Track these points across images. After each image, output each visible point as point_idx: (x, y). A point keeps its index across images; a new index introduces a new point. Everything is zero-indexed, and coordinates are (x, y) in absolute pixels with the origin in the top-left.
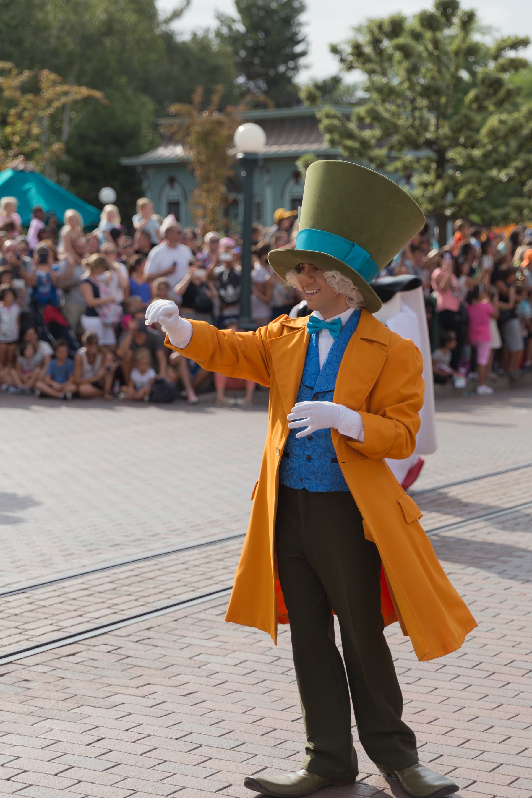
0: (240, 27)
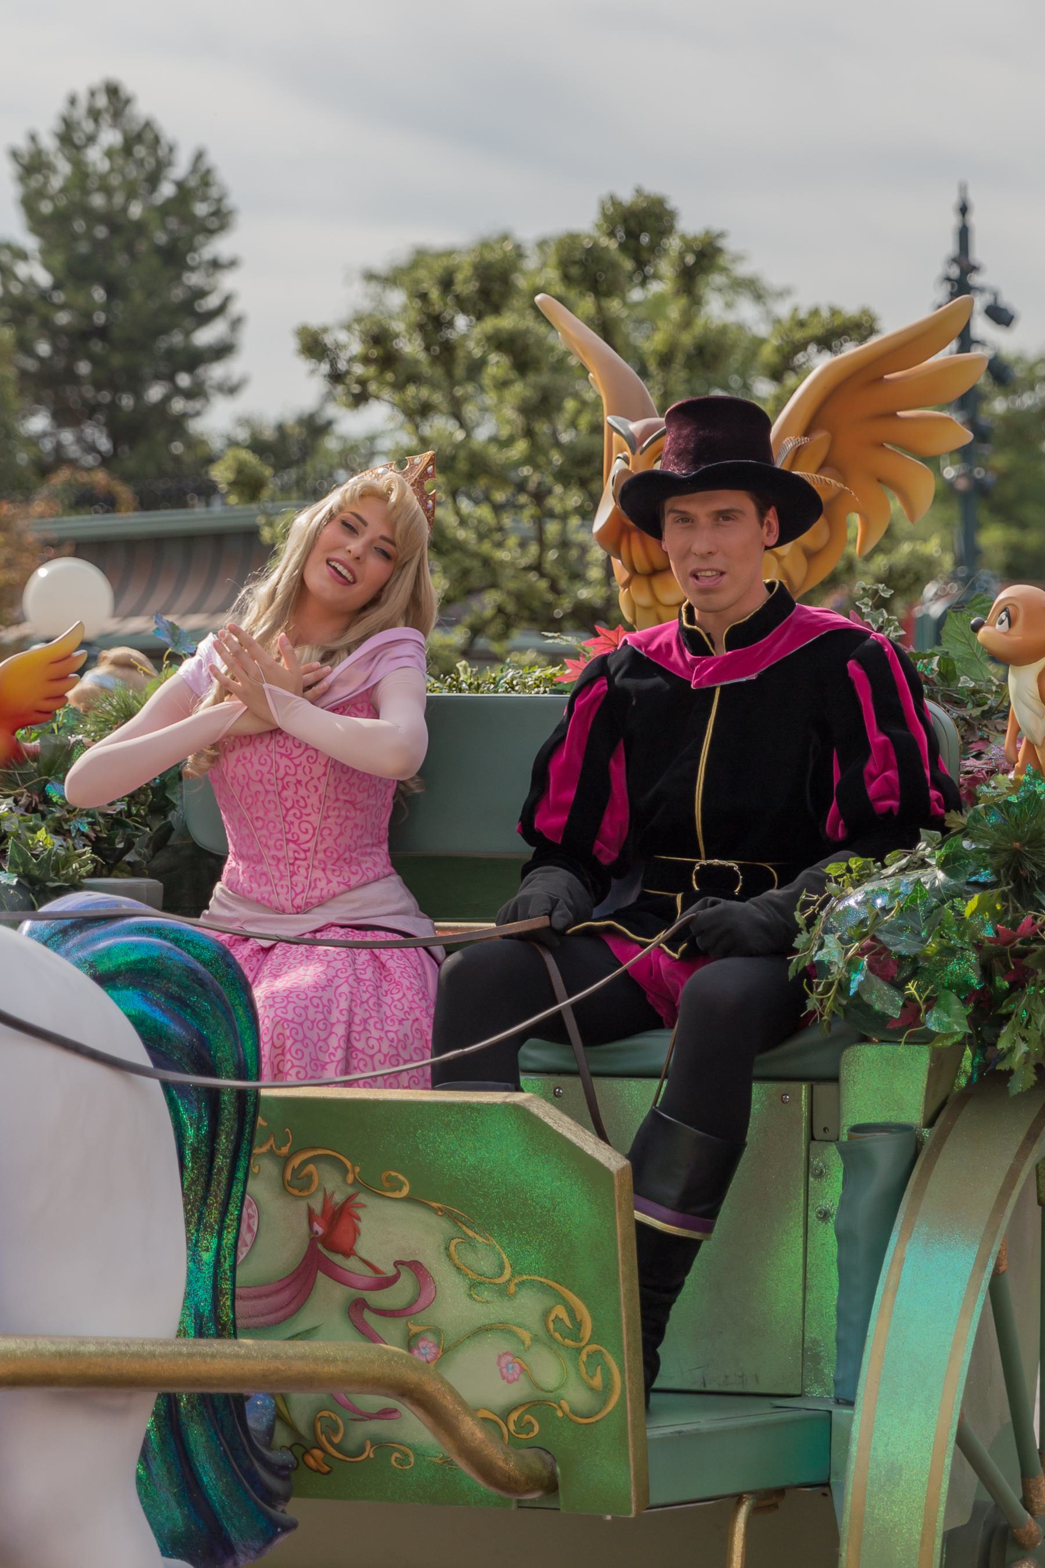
0: (37, 273)
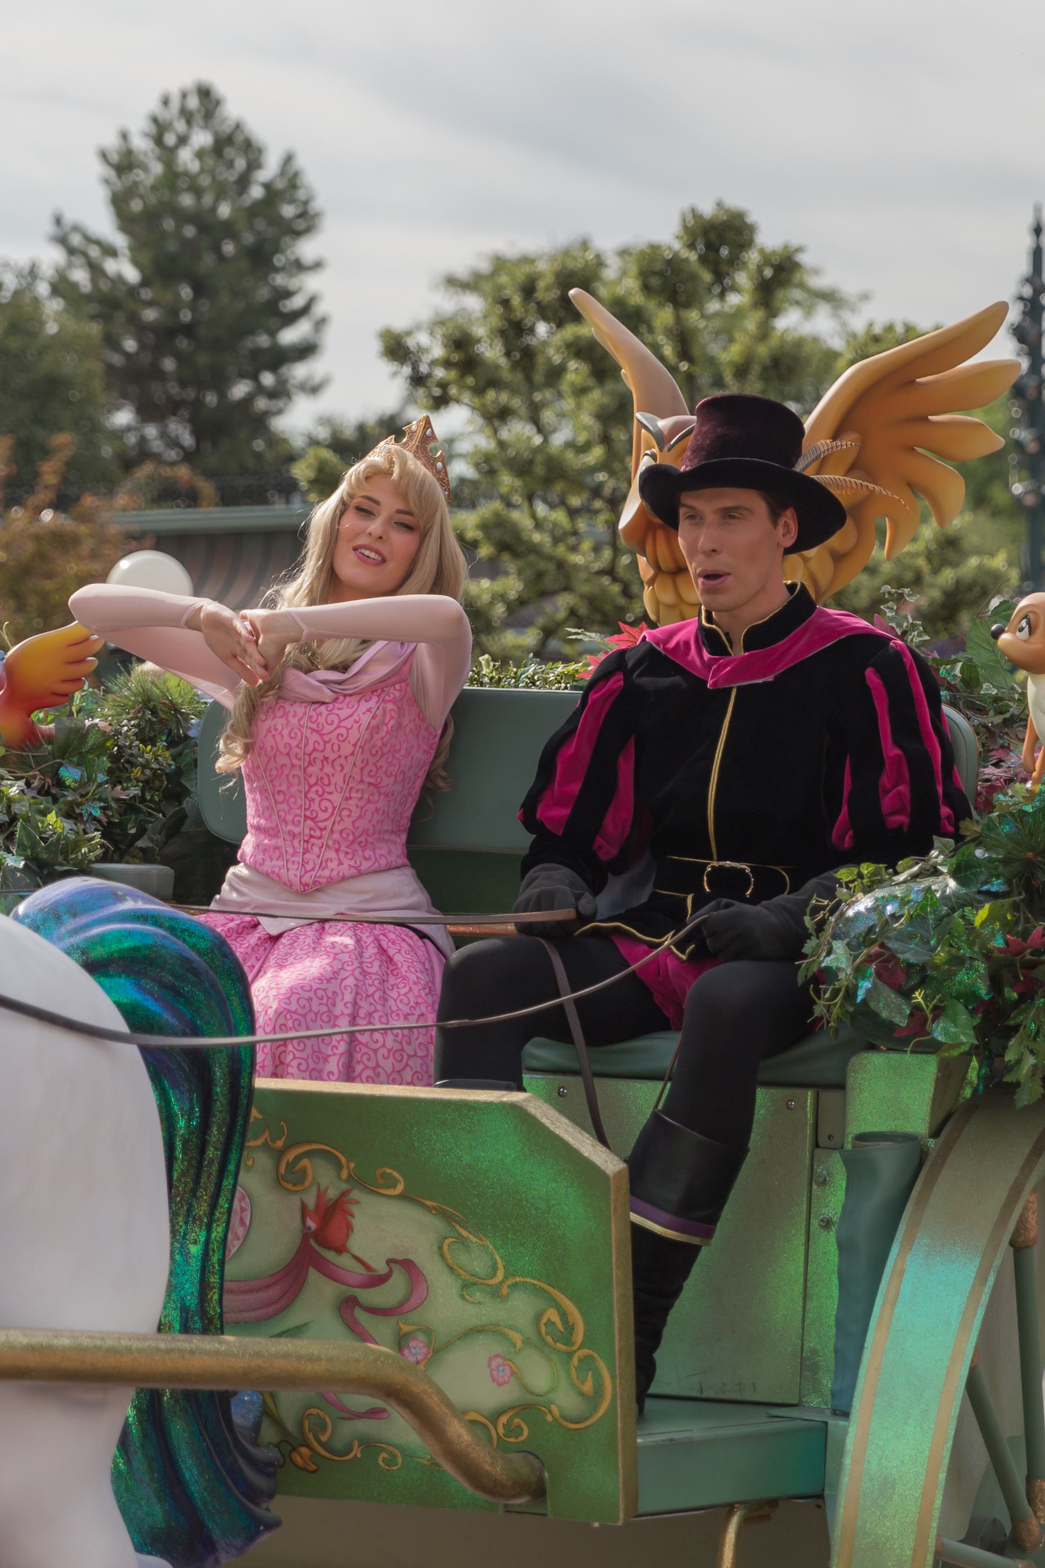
0: (126, 270)
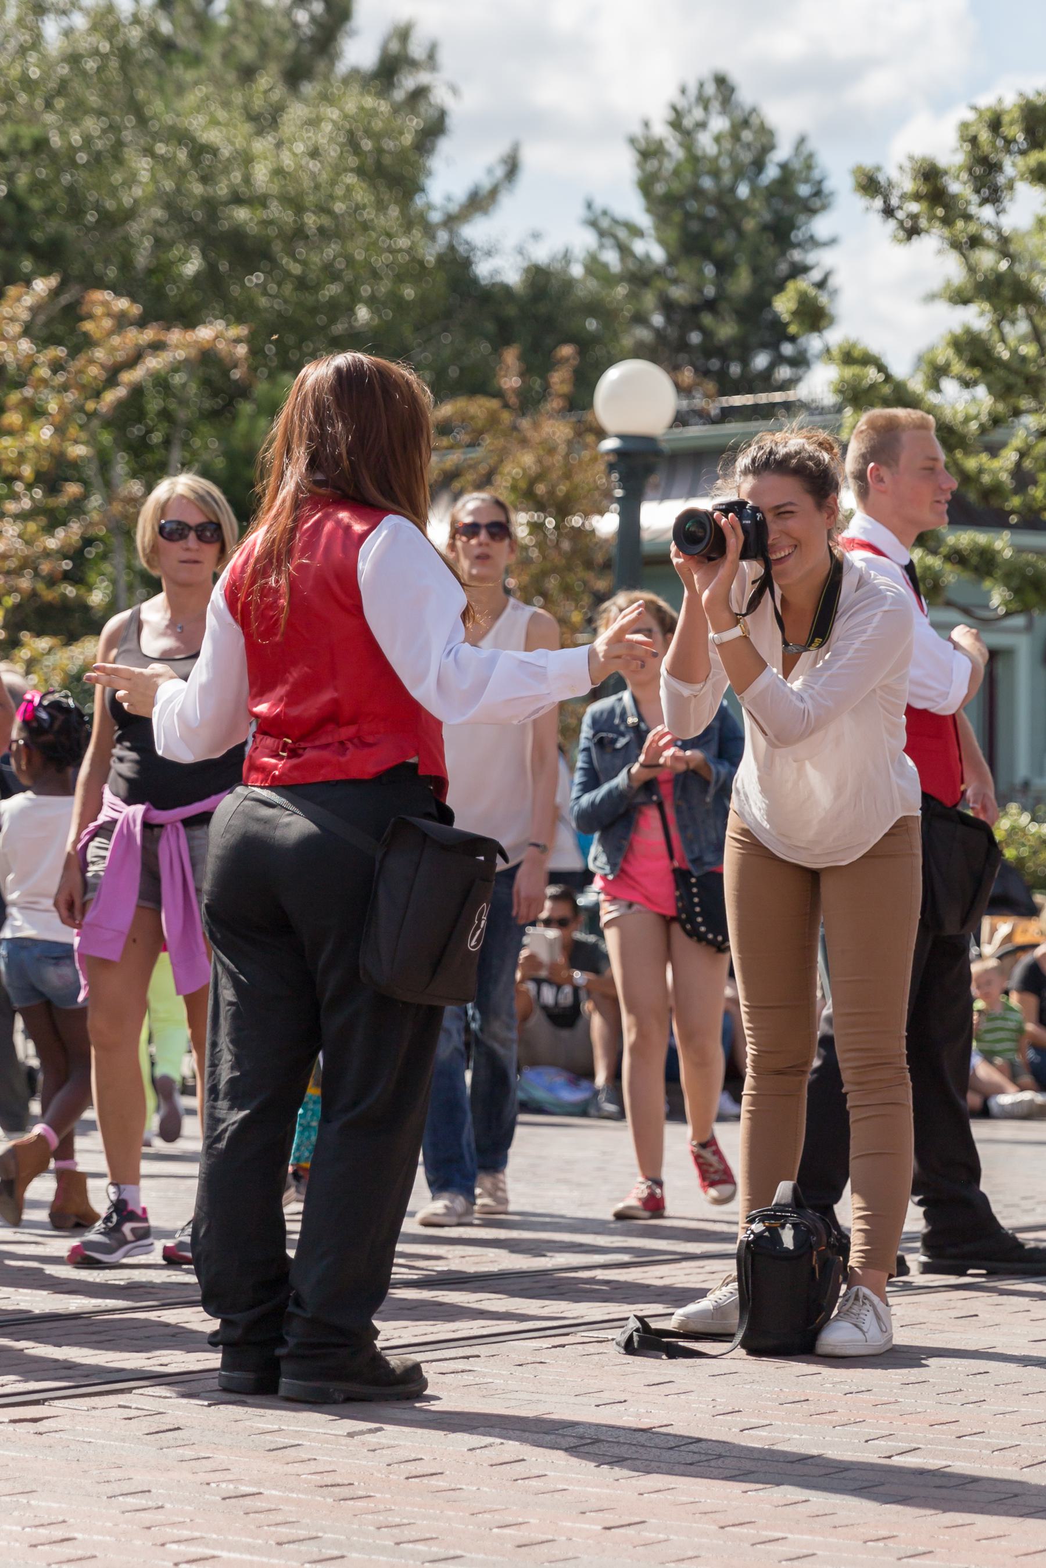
0: (652, 250)
